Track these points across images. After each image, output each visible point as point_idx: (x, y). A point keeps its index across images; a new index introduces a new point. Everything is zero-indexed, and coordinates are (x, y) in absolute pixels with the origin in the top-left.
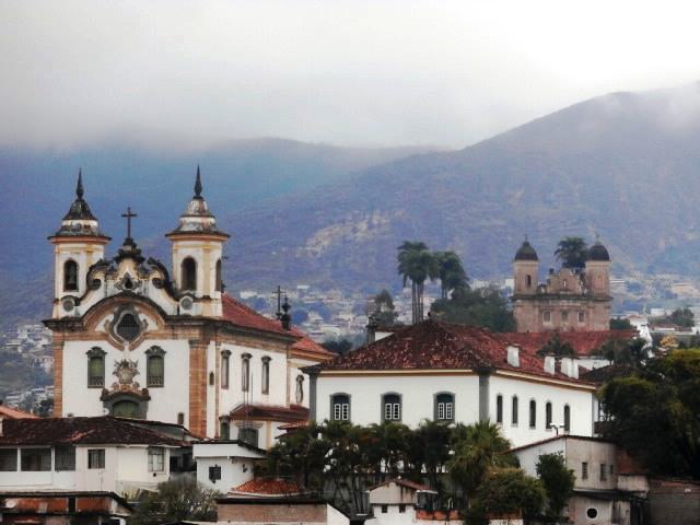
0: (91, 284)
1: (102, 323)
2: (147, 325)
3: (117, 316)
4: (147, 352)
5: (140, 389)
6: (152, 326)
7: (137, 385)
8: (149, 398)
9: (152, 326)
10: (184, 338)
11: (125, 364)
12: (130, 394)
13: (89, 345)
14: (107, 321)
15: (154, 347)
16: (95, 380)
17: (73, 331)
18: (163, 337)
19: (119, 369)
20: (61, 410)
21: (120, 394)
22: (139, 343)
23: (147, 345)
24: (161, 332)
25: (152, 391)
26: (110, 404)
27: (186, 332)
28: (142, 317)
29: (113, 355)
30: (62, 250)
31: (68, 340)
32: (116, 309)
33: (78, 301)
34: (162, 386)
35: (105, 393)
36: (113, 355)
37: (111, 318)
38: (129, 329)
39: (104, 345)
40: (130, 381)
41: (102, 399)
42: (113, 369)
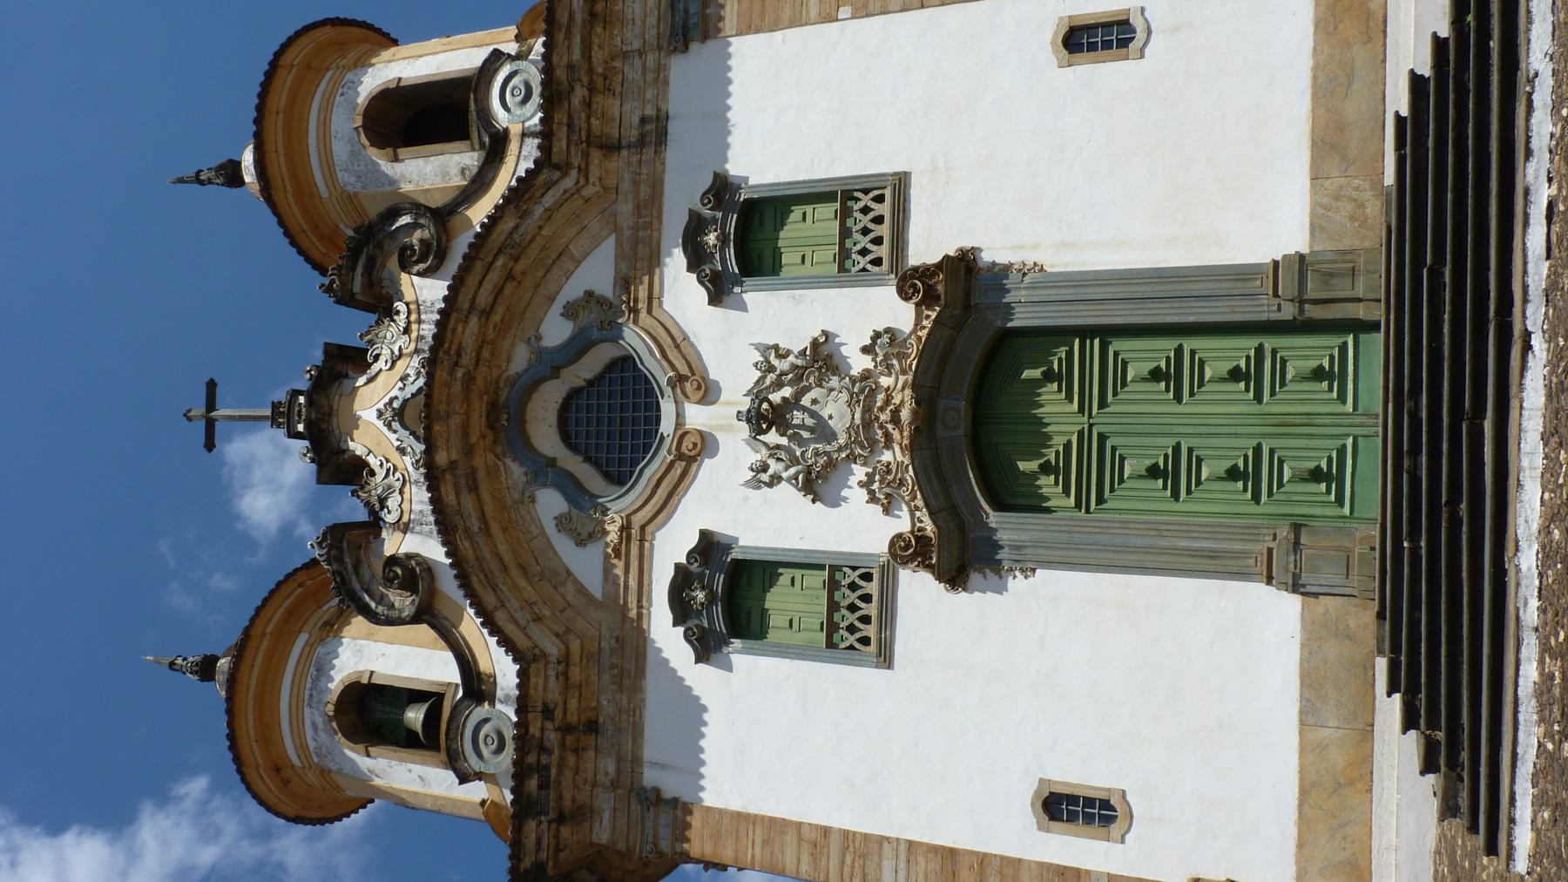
0: (404, 602)
1: (563, 545)
2: (589, 294)
3: (544, 471)
4: (719, 291)
5: (899, 314)
6: (596, 272)
7: (885, 342)
8: (963, 265)
9: (596, 272)
10: (660, 79)
11: (763, 417)
12: (927, 392)
13: (667, 638)
14: (562, 522)
15: (697, 259)
16: (854, 620)
17: (593, 727)
18: (650, 204)
19: (794, 461)
20: (1012, 866)
21: (924, 440)
22: (675, 343)
23: (680, 290)
24: (625, 209)
25: (927, 244)
26: (1005, 526)
27: (633, 71)
28: (556, 331)
29: (730, 498)
30: (302, 747)
31: (637, 761)
32: (516, 471)
33: (477, 686)
34: (901, 183)
35: (910, 550)
36: (730, 498)
37: (550, 503)
38: (622, 422)
39: (672, 546)
40: (864, 390)
41: (955, 578)
42: (788, 495)
